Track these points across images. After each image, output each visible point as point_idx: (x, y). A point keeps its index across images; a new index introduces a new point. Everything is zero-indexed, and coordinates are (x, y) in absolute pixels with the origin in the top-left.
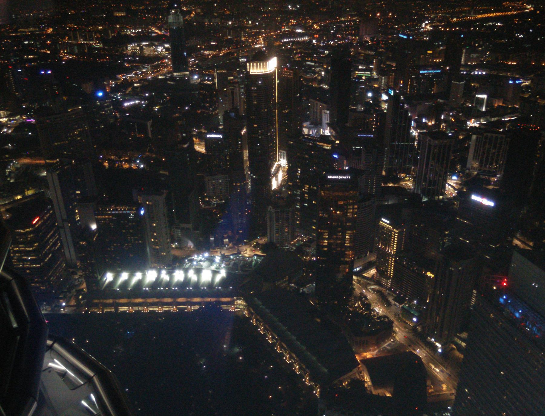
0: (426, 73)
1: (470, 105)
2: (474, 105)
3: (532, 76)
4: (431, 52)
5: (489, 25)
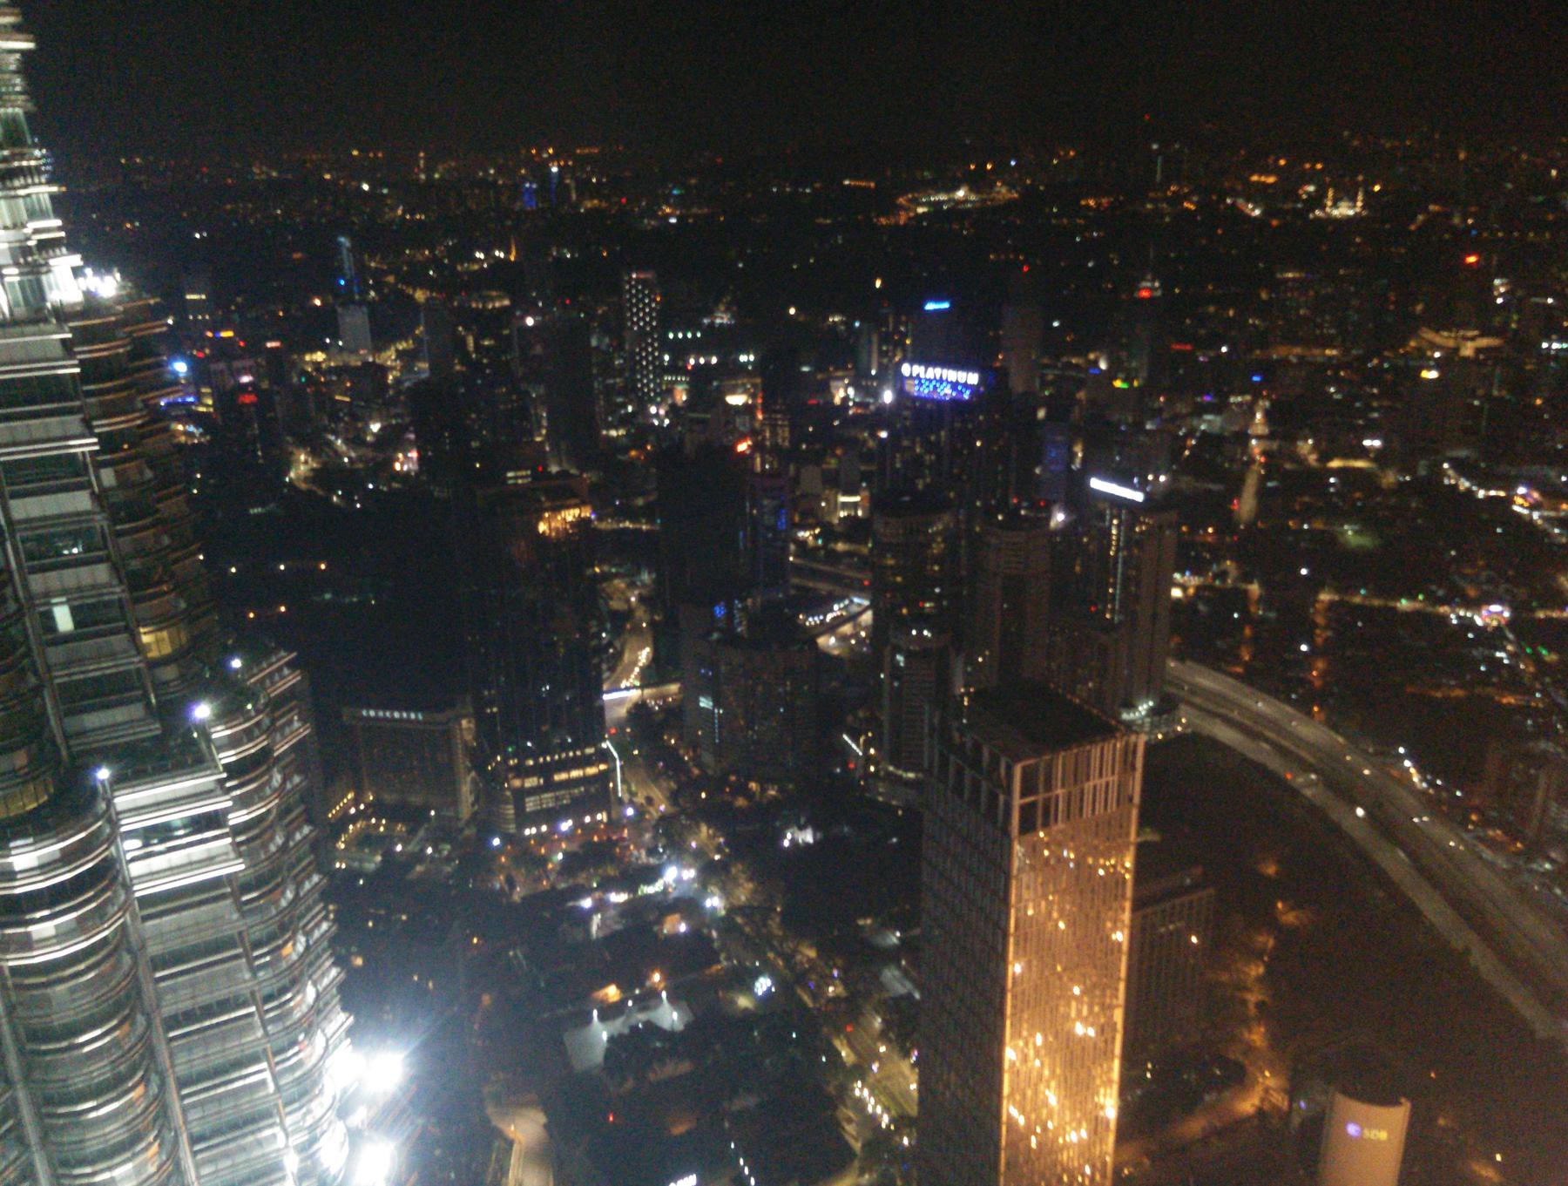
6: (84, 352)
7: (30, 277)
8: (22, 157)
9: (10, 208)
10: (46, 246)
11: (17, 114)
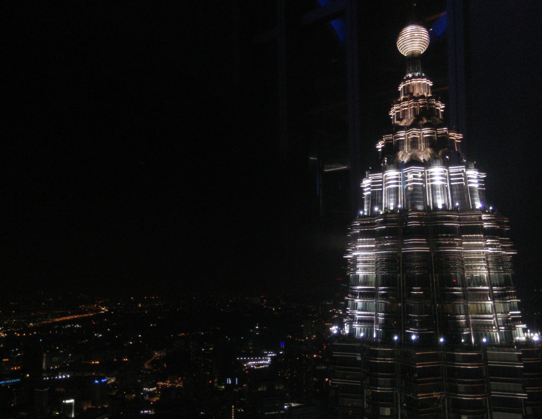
0: (4, 384)
1: (57, 413)
2: (62, 412)
3: (116, 372)
4: (7, 360)
5: (68, 328)
6: (525, 360)
7: (508, 331)
8: (509, 289)
9: (504, 305)
10: (516, 320)
11: (509, 275)
